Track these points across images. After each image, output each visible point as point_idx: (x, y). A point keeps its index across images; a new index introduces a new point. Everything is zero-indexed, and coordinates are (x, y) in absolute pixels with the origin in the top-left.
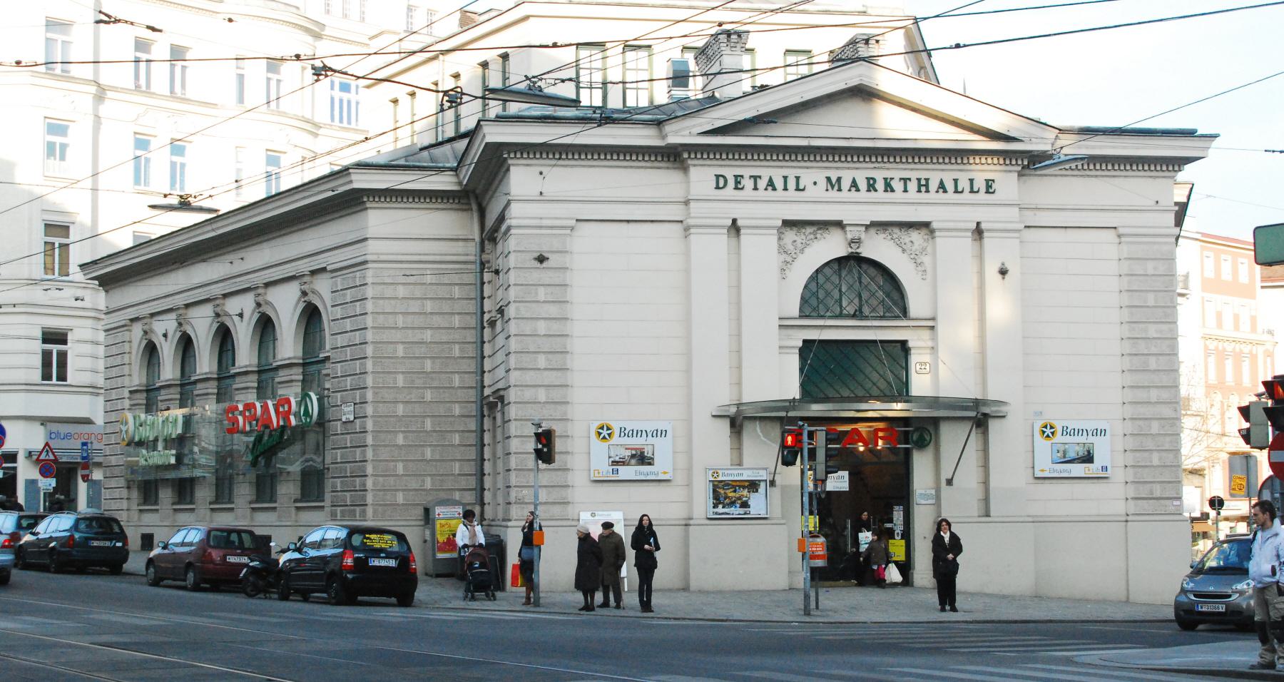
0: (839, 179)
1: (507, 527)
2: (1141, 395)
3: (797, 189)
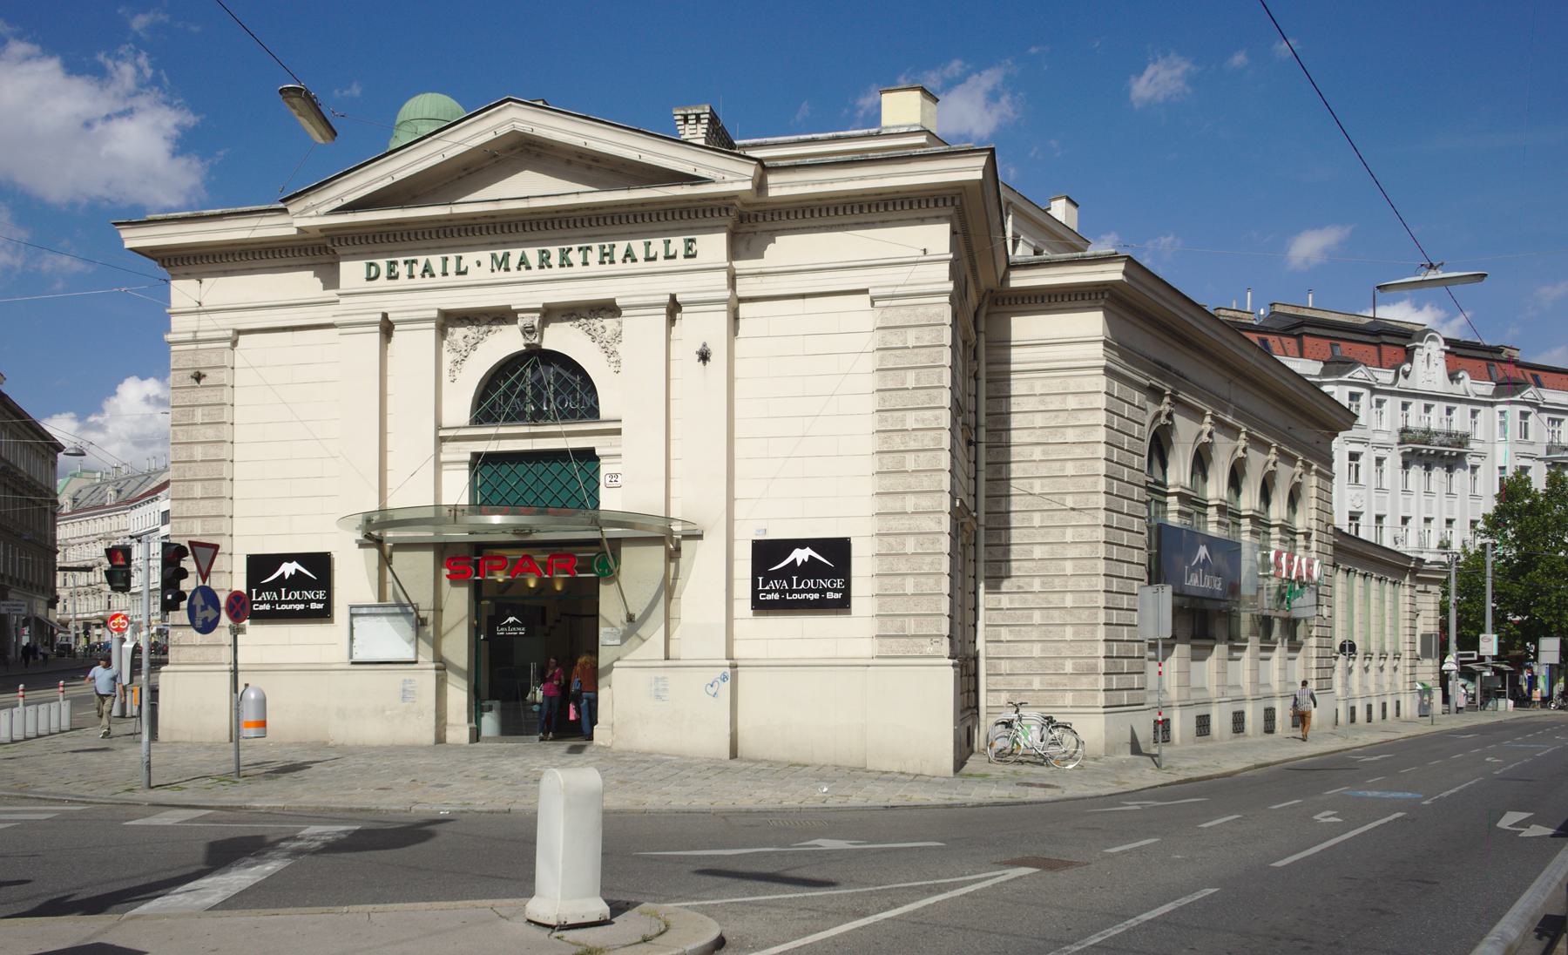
2: (894, 504)
3: (459, 273)
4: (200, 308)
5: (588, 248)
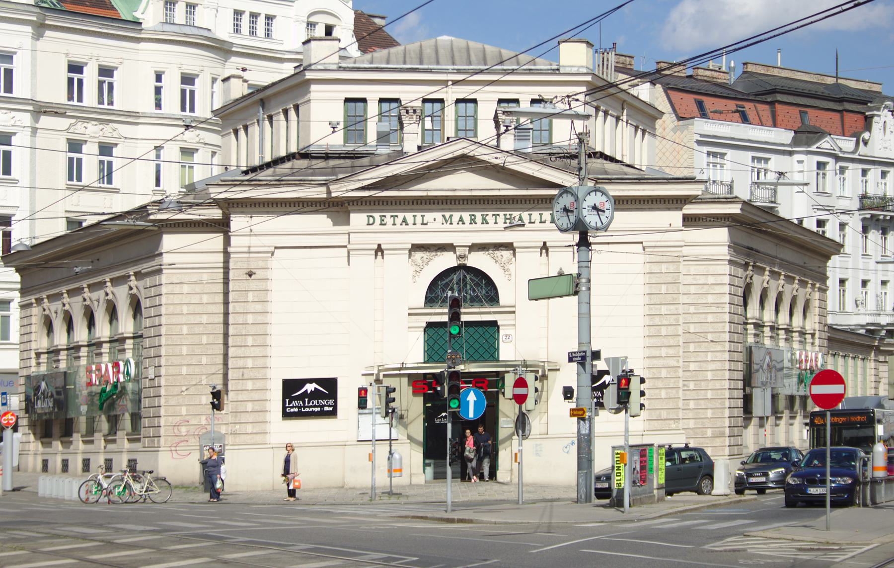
1: (158, 451)
4: (252, 233)
5: (498, 215)
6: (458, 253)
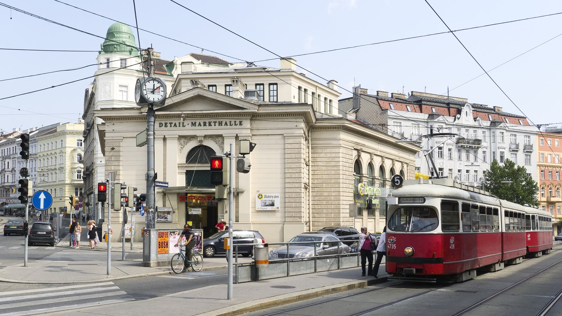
0: (195, 123)
3: (183, 126)
6: (199, 139)
